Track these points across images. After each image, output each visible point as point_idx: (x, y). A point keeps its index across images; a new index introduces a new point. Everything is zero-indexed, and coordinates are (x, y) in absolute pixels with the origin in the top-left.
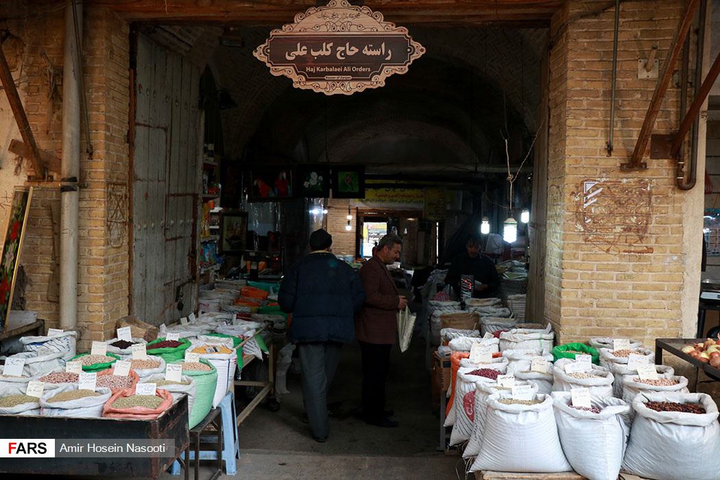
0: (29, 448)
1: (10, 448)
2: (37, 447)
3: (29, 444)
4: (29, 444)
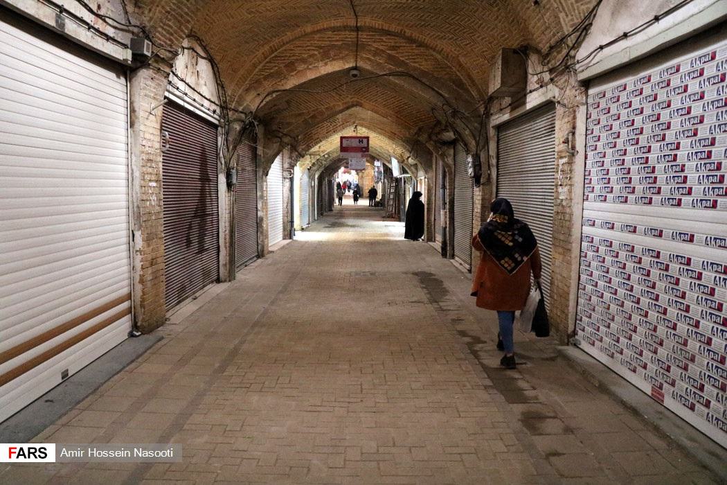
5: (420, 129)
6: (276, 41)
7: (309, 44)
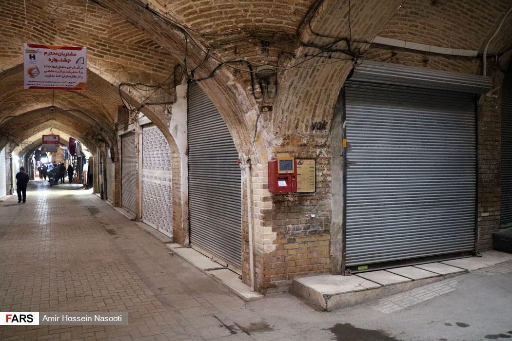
0: (21, 318)
1: (7, 318)
2: (27, 317)
3: (21, 315)
4: (21, 315)
5: (87, 133)
6: (10, 92)
7: (28, 93)
